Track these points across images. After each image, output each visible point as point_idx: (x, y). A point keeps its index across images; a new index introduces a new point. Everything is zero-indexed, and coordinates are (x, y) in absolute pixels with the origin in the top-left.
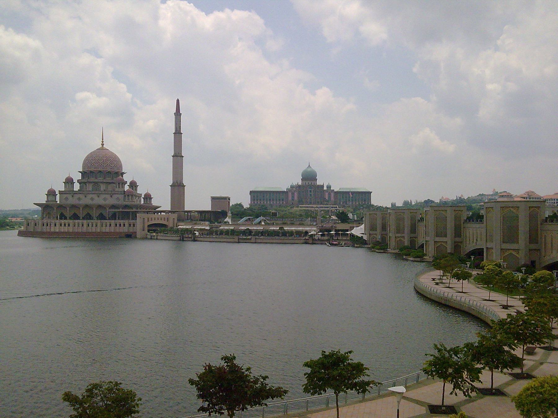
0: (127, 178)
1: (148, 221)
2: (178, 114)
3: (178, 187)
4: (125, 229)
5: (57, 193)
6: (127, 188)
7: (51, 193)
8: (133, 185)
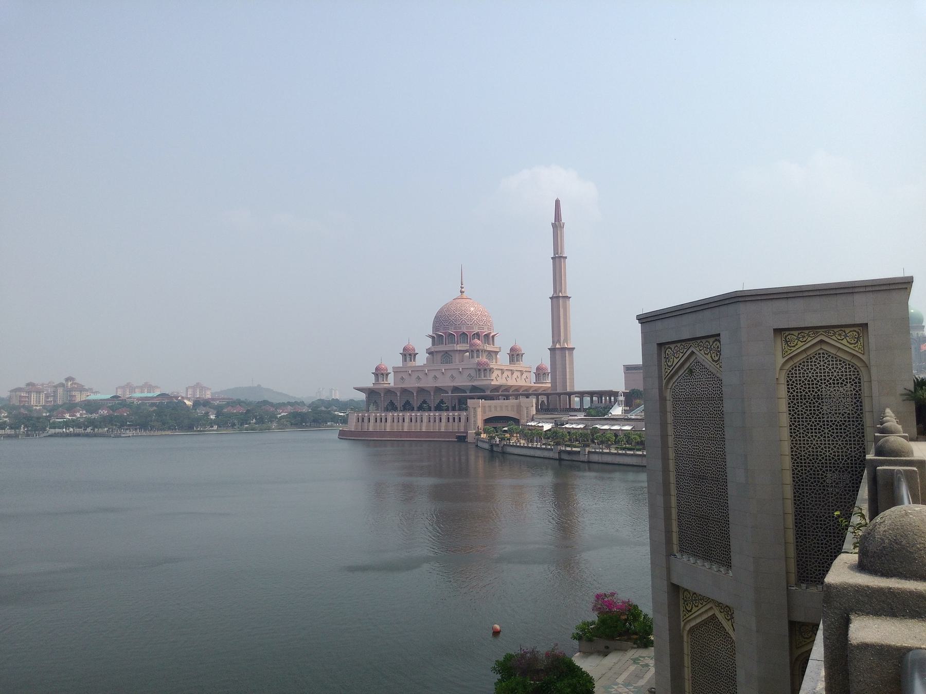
0: (503, 344)
1: (484, 412)
2: (557, 225)
3: (560, 352)
4: (454, 427)
5: (390, 370)
6: (503, 359)
7: (380, 373)
8: (515, 355)
